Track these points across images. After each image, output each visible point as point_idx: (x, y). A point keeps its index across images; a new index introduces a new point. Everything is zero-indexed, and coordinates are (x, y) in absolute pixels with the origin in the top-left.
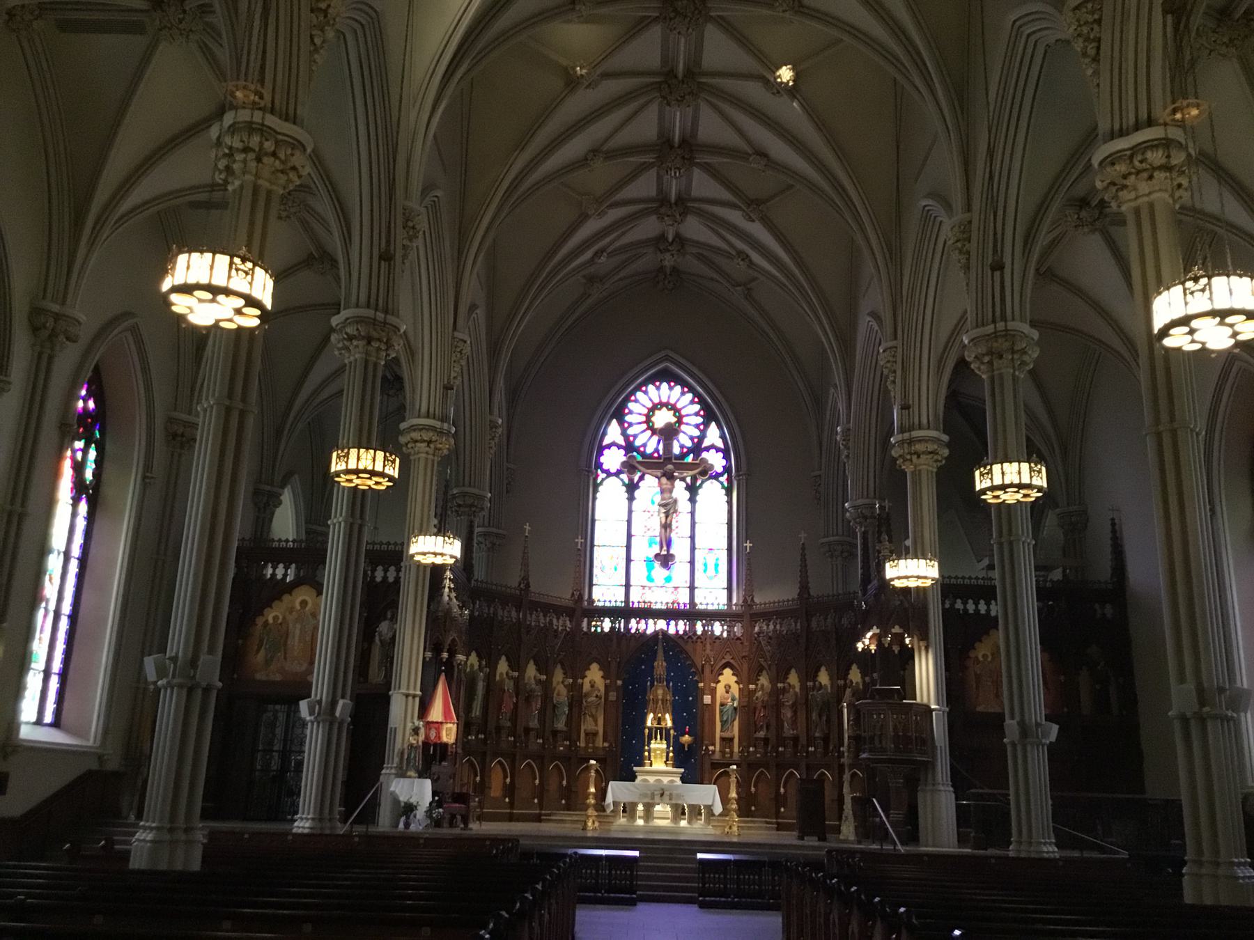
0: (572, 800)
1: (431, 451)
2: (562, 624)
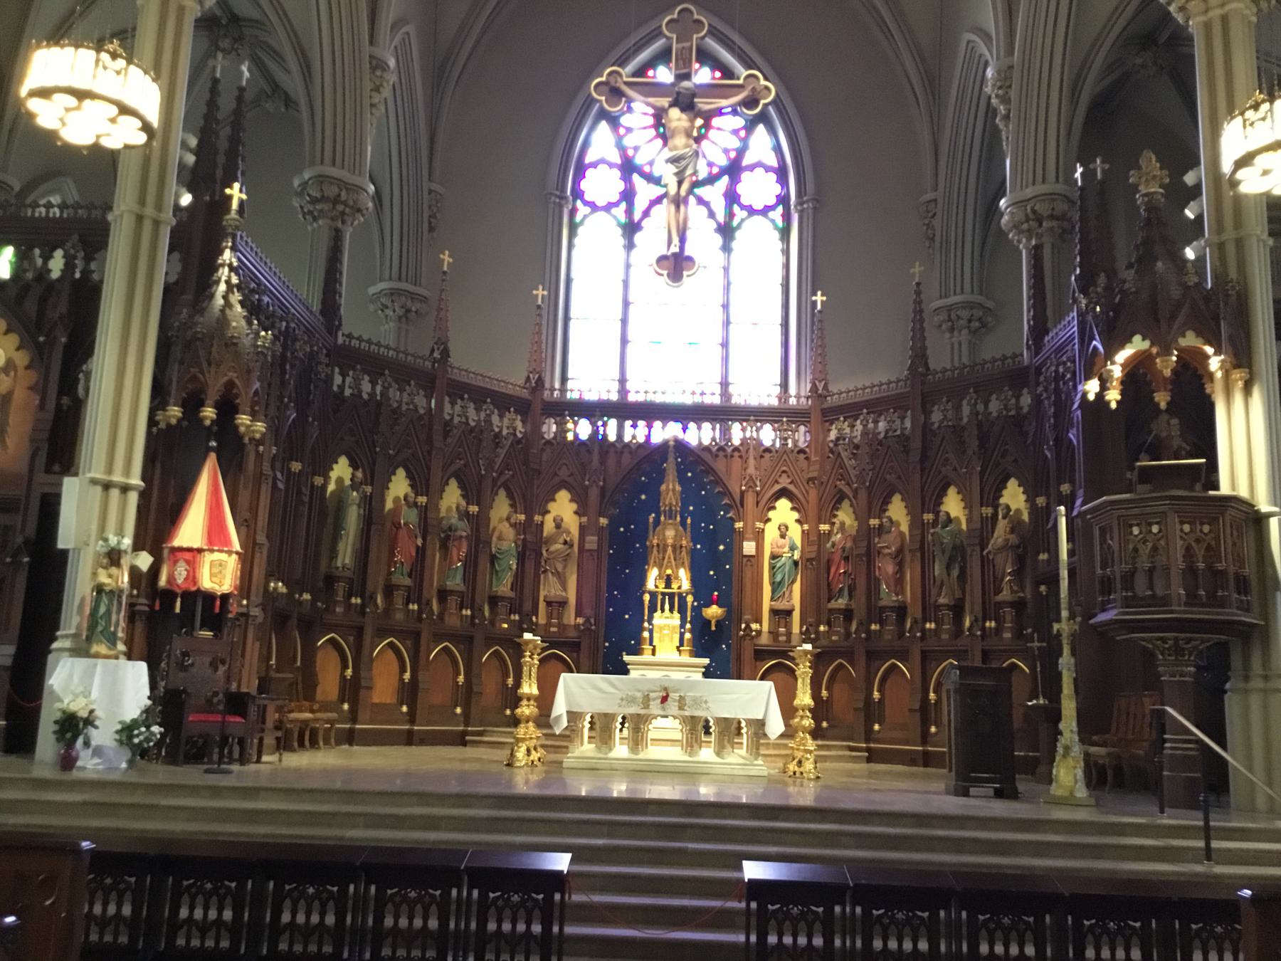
0: (488, 709)
2: (510, 424)
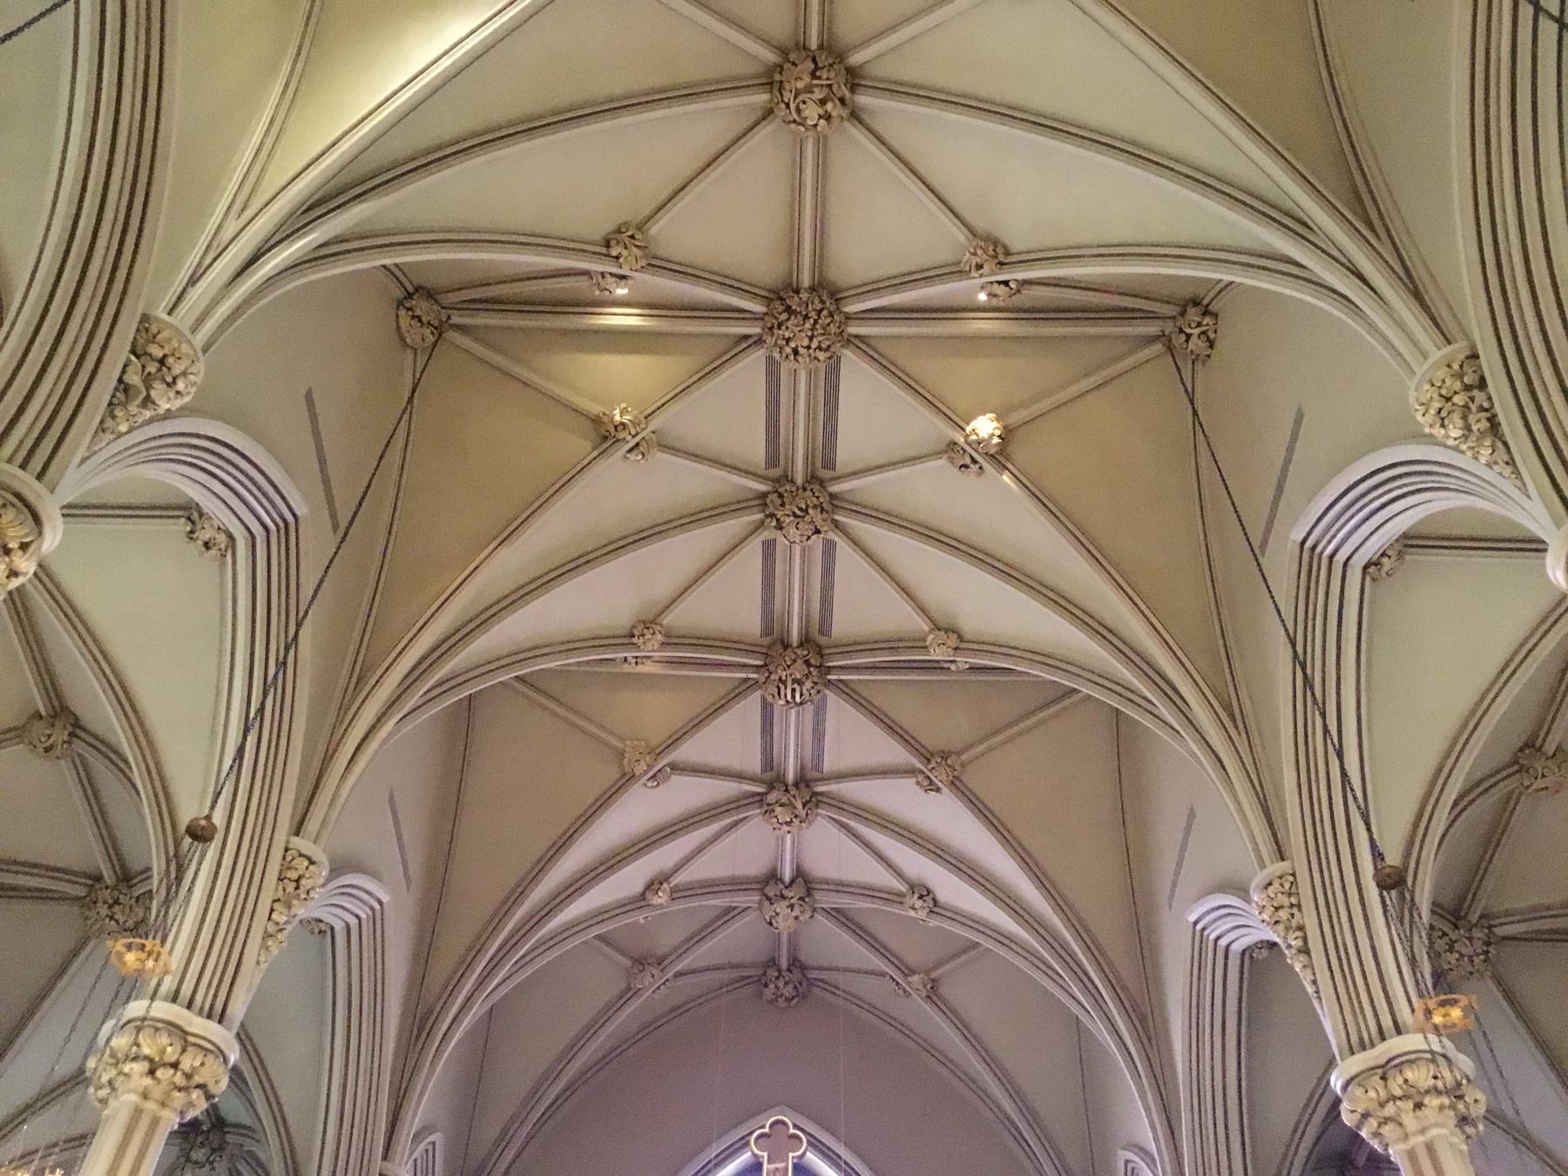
1: (157, 1093)
